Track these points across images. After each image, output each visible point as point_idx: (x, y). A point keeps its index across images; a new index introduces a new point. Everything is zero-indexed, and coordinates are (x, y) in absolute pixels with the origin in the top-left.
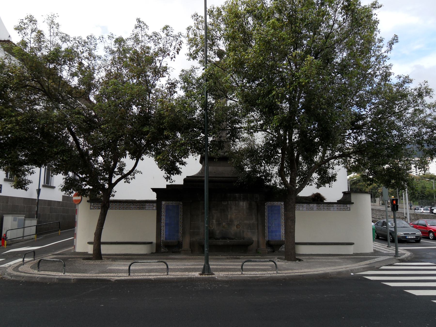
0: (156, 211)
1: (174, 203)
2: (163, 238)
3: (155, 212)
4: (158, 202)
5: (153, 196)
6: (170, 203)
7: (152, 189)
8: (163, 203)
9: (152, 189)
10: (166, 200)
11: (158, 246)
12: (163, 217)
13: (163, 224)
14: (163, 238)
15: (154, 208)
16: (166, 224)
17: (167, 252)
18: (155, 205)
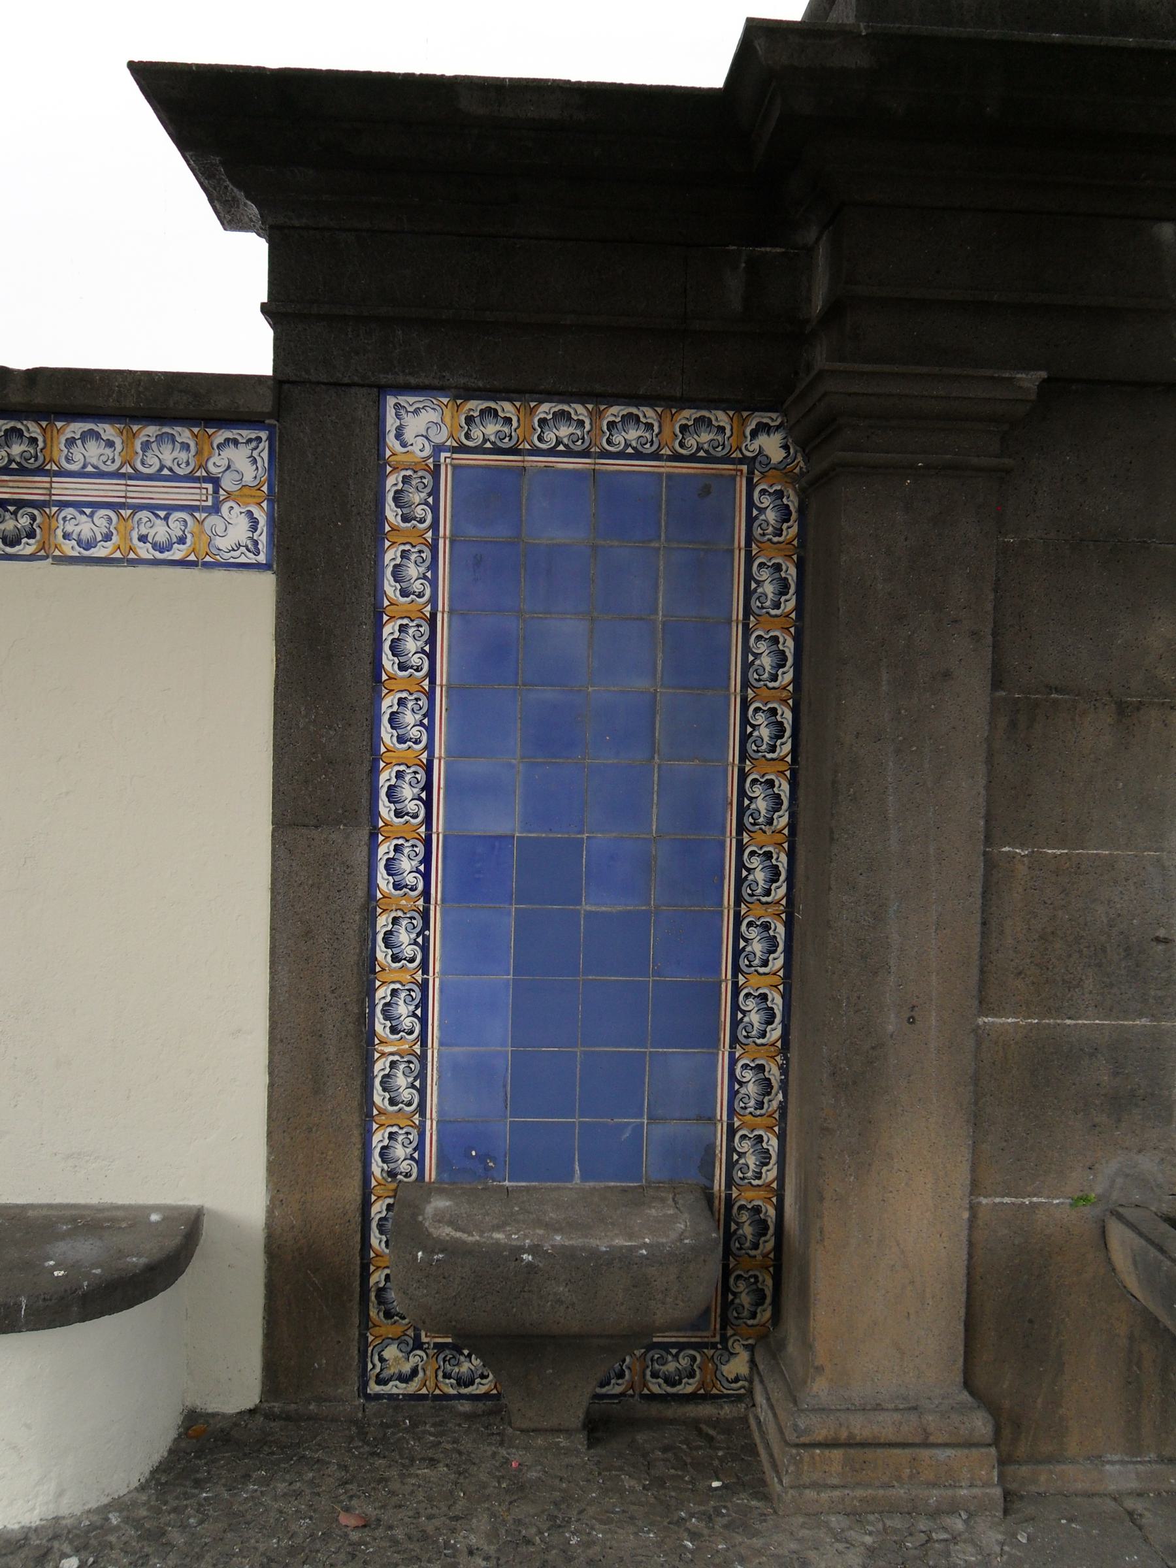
0: (261, 593)
1: (631, 438)
2: (411, 1115)
3: (238, 628)
4: (305, 415)
5: (201, 296)
6: (554, 431)
7: (157, 81)
8: (418, 426)
9: (157, 81)
10: (489, 359)
11: (317, 1286)
12: (409, 730)
13: (396, 867)
14: (411, 1115)
15: (237, 529)
16: (475, 867)
17: (492, 1408)
18: (243, 460)
